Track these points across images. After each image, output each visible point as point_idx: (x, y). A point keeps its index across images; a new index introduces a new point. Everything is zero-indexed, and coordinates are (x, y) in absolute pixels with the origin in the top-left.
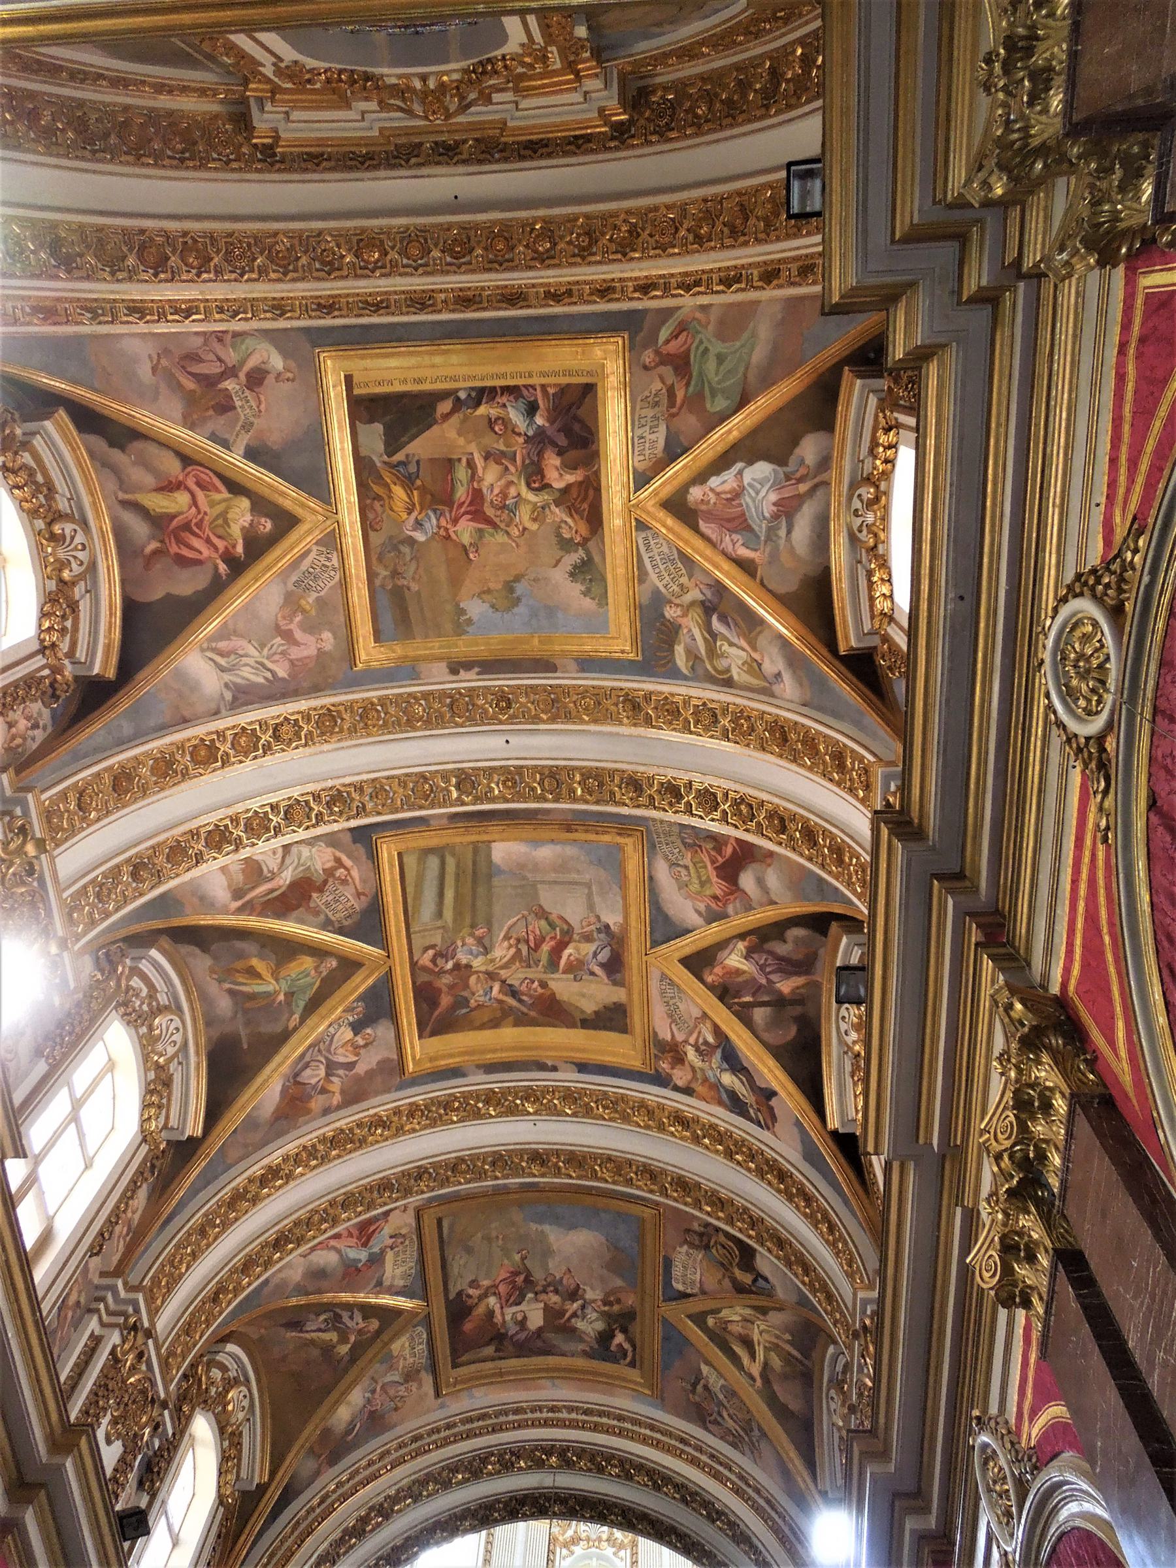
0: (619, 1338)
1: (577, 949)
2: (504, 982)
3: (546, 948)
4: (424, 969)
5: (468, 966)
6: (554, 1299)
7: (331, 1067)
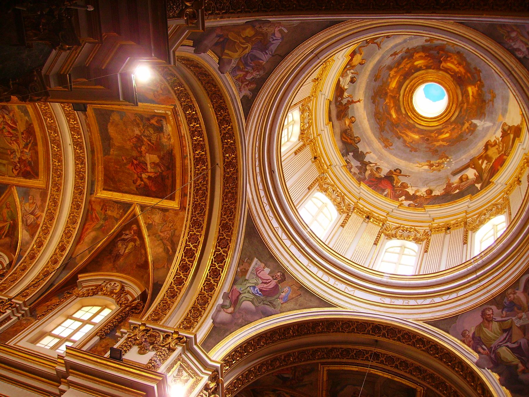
0: (153, 121)
1: (9, 120)
2: (24, 148)
3: (11, 131)
4: (18, 174)
5: (19, 159)
6: (143, 148)
7: (32, 213)
